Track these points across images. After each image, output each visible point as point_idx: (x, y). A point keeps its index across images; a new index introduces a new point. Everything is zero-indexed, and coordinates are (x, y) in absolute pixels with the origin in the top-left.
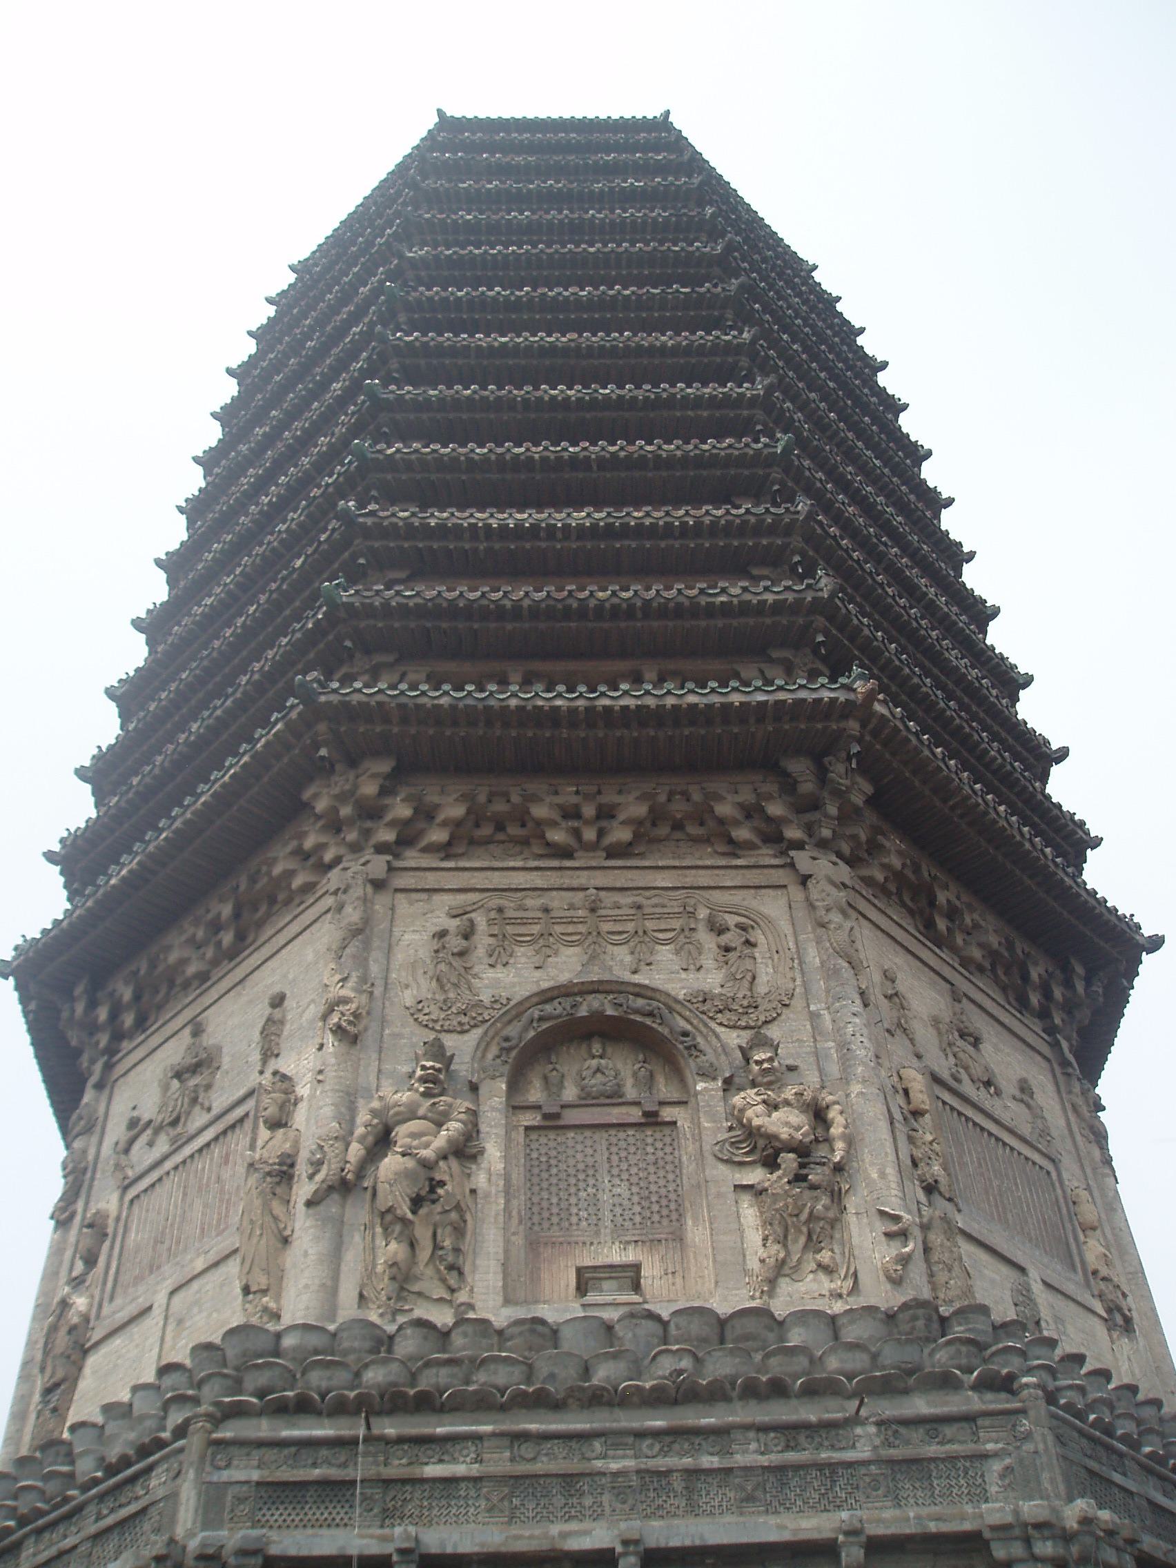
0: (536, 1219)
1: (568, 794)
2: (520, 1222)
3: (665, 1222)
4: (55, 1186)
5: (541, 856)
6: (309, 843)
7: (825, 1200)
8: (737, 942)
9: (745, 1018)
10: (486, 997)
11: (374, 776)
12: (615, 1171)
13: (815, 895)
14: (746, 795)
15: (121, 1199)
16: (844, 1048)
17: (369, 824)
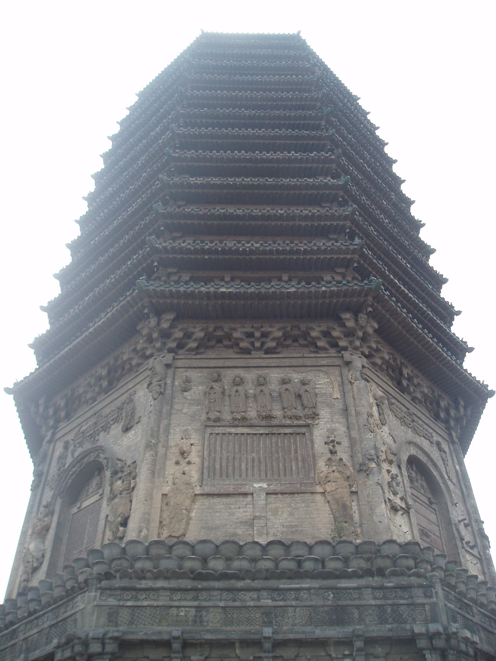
5: (238, 353)
6: (139, 347)
11: (167, 320)
14: (324, 328)
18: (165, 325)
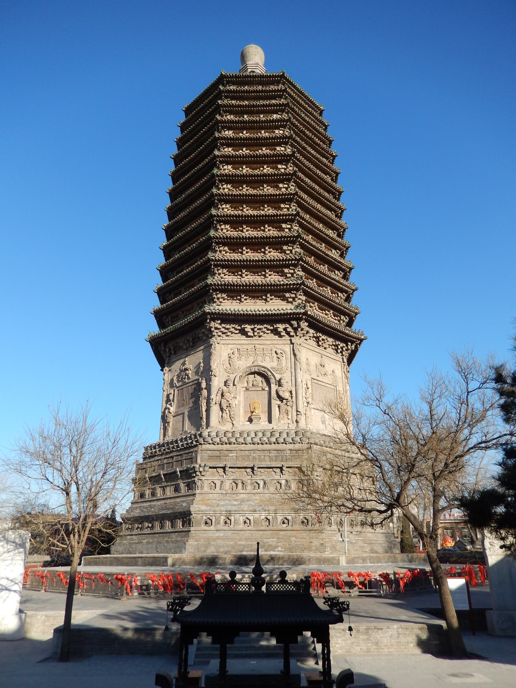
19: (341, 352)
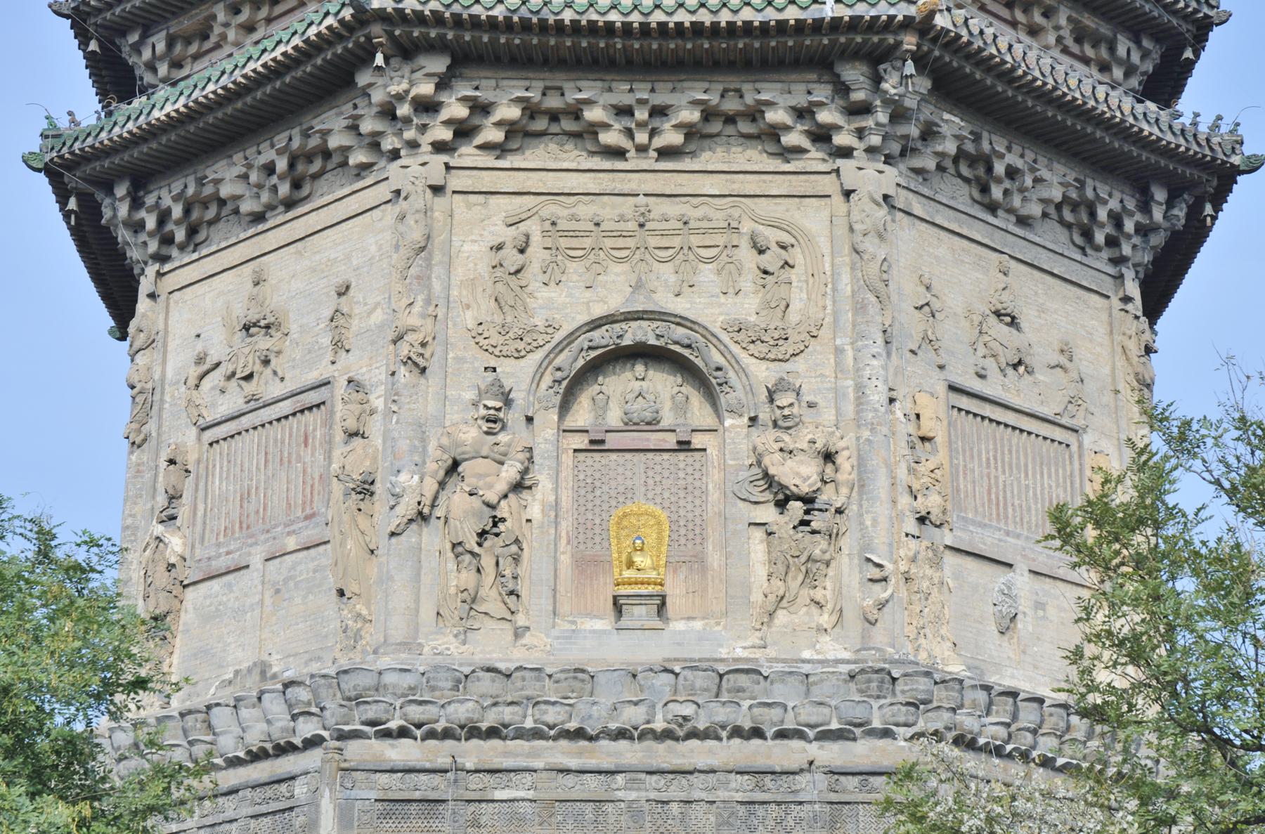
0: (581, 538)
1: (622, 93)
2: (568, 542)
3: (690, 545)
4: (121, 408)
7: (824, 544)
8: (774, 261)
9: (774, 350)
10: (539, 321)
12: (650, 495)
13: (856, 216)
15: (199, 439)
16: (860, 390)
17: (425, 119)
18: (426, 88)
19: (1112, 242)
